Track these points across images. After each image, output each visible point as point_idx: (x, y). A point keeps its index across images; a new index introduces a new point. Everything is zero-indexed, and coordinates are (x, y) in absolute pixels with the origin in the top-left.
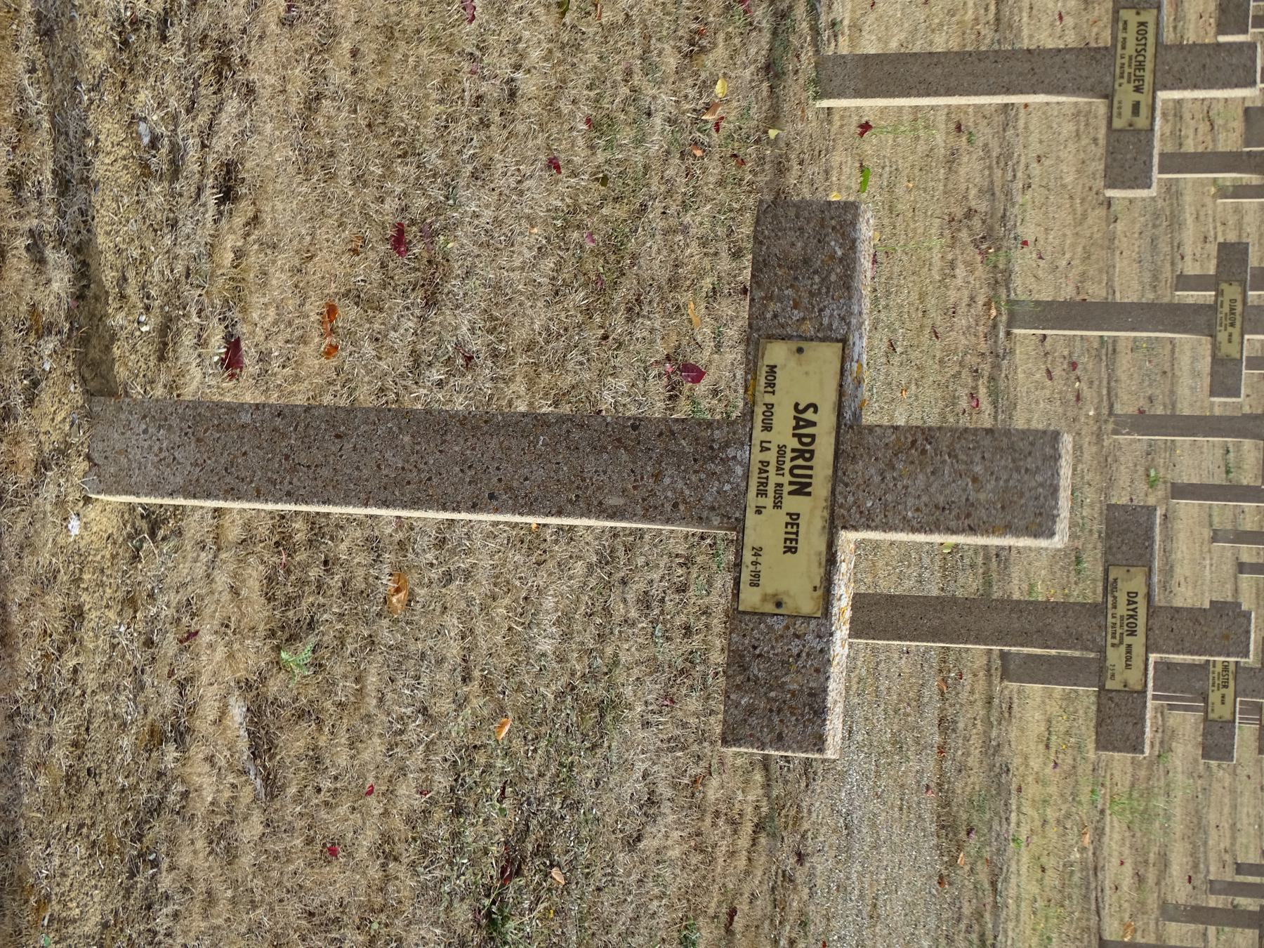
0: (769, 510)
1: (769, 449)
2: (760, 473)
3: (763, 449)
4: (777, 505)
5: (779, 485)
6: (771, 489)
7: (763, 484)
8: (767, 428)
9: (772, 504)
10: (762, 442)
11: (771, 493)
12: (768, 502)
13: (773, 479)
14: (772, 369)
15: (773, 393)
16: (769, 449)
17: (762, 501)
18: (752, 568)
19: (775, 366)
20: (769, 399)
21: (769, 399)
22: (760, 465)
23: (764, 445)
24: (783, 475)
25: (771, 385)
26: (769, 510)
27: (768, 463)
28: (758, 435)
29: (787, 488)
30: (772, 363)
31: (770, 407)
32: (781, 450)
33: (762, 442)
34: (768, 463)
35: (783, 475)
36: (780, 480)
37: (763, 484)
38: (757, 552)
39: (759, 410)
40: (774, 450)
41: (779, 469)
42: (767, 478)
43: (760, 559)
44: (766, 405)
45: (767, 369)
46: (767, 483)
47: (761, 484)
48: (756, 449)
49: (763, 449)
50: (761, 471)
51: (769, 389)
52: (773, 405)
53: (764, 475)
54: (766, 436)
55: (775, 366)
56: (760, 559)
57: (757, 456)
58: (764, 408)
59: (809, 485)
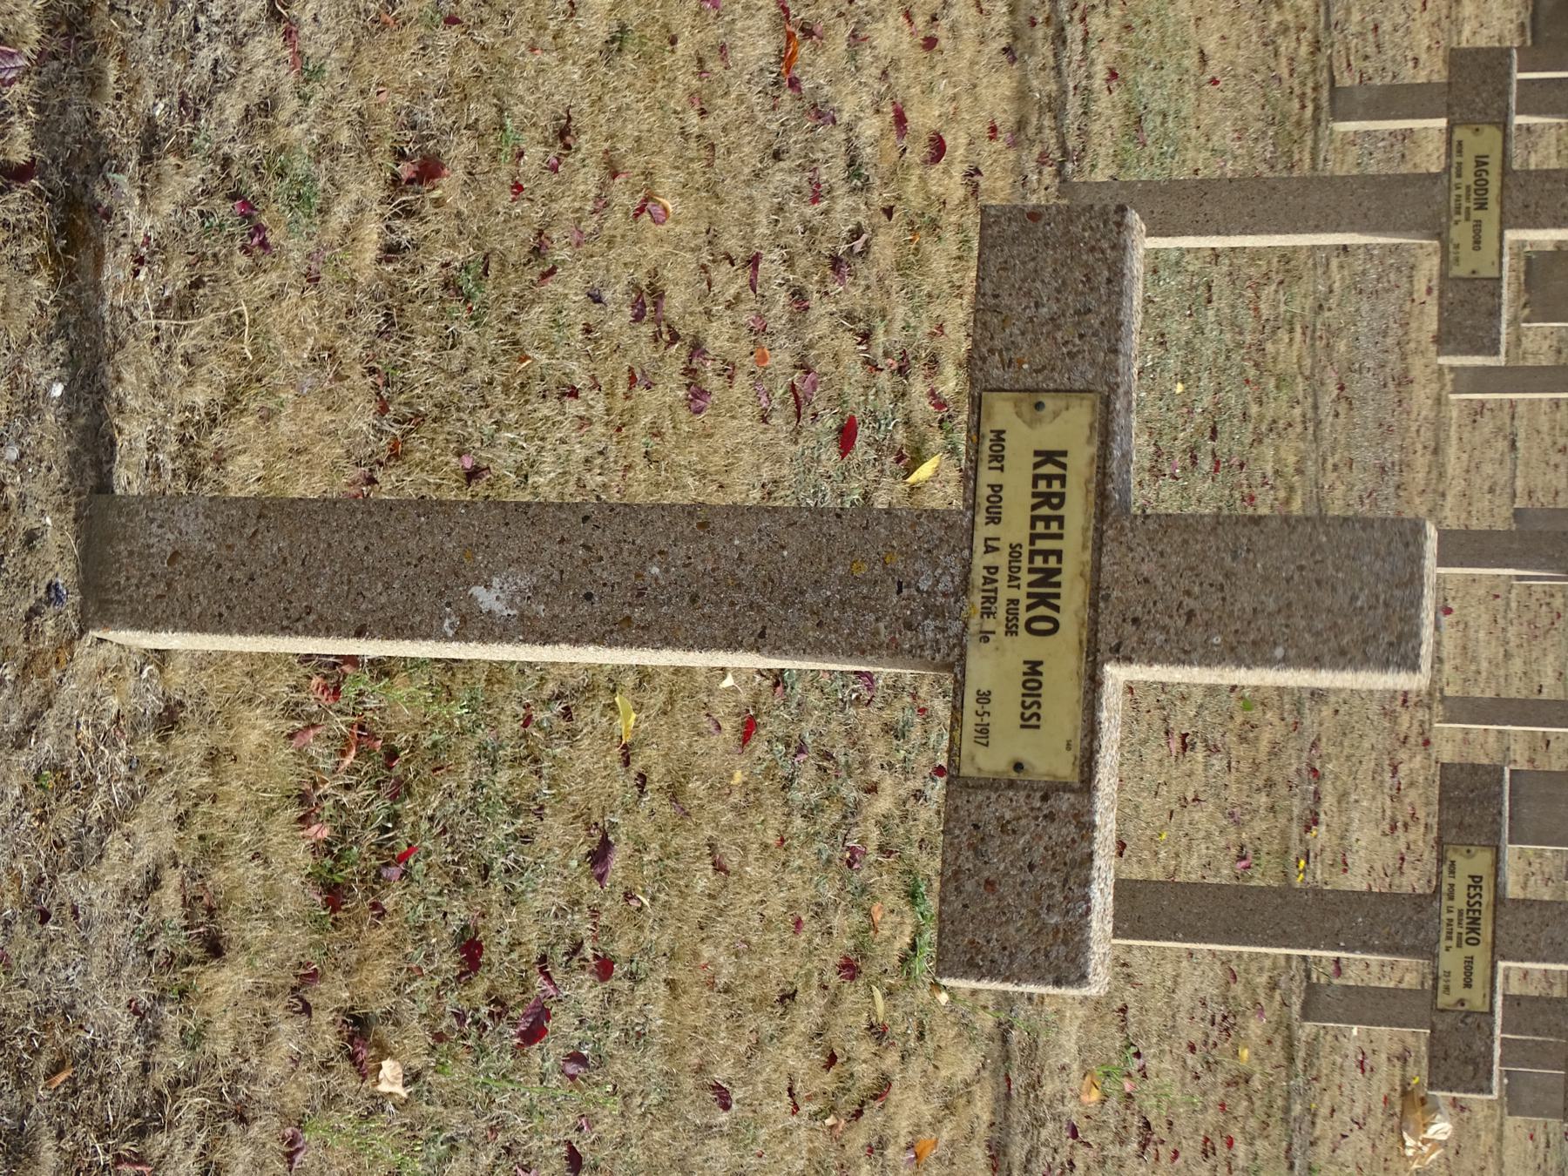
1: (996, 549)
3: (989, 549)
4: (1011, 631)
8: (994, 519)
10: (986, 540)
11: (1002, 613)
13: (1005, 593)
14: (999, 436)
15: (1002, 469)
16: (996, 549)
17: (989, 624)
18: (978, 720)
22: (985, 573)
24: (1018, 587)
25: (998, 457)
27: (997, 568)
28: (983, 531)
29: (1024, 602)
30: (998, 427)
31: (996, 489)
32: (1015, 550)
33: (986, 540)
34: (997, 568)
35: (1018, 587)
36: (1014, 594)
38: (984, 697)
39: (984, 491)
41: (1011, 578)
42: (995, 590)
43: (987, 708)
44: (992, 486)
45: (992, 436)
48: (979, 547)
49: (989, 549)
50: (987, 581)
51: (995, 464)
52: (1001, 486)
54: (992, 530)
57: (980, 561)
58: (989, 491)
59: (1057, 596)
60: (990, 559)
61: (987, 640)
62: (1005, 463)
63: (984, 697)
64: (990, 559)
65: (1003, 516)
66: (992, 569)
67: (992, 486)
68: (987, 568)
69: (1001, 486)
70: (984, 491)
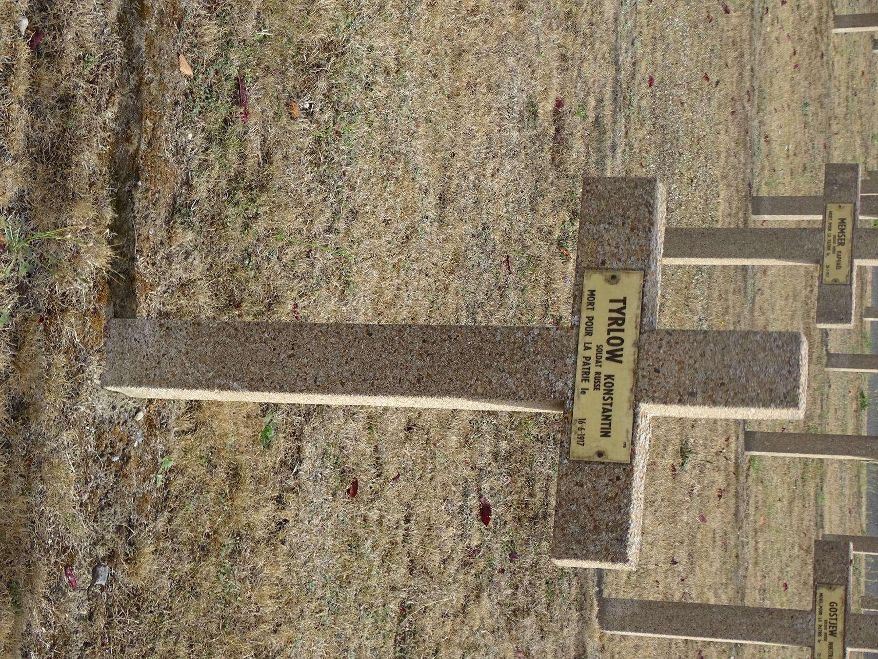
0: (591, 392)
1: (590, 348)
2: (584, 365)
4: (596, 388)
5: (599, 373)
6: (592, 376)
7: (586, 373)
8: (589, 333)
9: (593, 387)
10: (585, 343)
12: (590, 385)
13: (594, 369)
14: (592, 293)
15: (593, 309)
16: (590, 348)
17: (585, 385)
19: (594, 291)
20: (590, 313)
21: (590, 313)
22: (584, 360)
23: (587, 345)
24: (601, 366)
25: (591, 303)
26: (591, 392)
27: (590, 358)
28: (583, 339)
30: (593, 289)
31: (591, 319)
32: (599, 349)
33: (585, 343)
34: (590, 358)
37: (586, 373)
39: (584, 320)
40: (594, 348)
41: (597, 362)
42: (589, 369)
43: (584, 426)
44: (588, 317)
45: (589, 293)
46: (589, 373)
47: (585, 373)
48: (581, 347)
50: (585, 364)
51: (590, 307)
52: (593, 318)
53: (587, 367)
54: (588, 339)
55: (594, 291)
56: (584, 426)
58: (587, 320)
60: (588, 353)
61: (584, 393)
62: (595, 306)
63: (582, 421)
64: (588, 353)
65: (594, 332)
66: (588, 358)
67: (588, 317)
68: (585, 358)
69: (593, 318)
70: (584, 320)
